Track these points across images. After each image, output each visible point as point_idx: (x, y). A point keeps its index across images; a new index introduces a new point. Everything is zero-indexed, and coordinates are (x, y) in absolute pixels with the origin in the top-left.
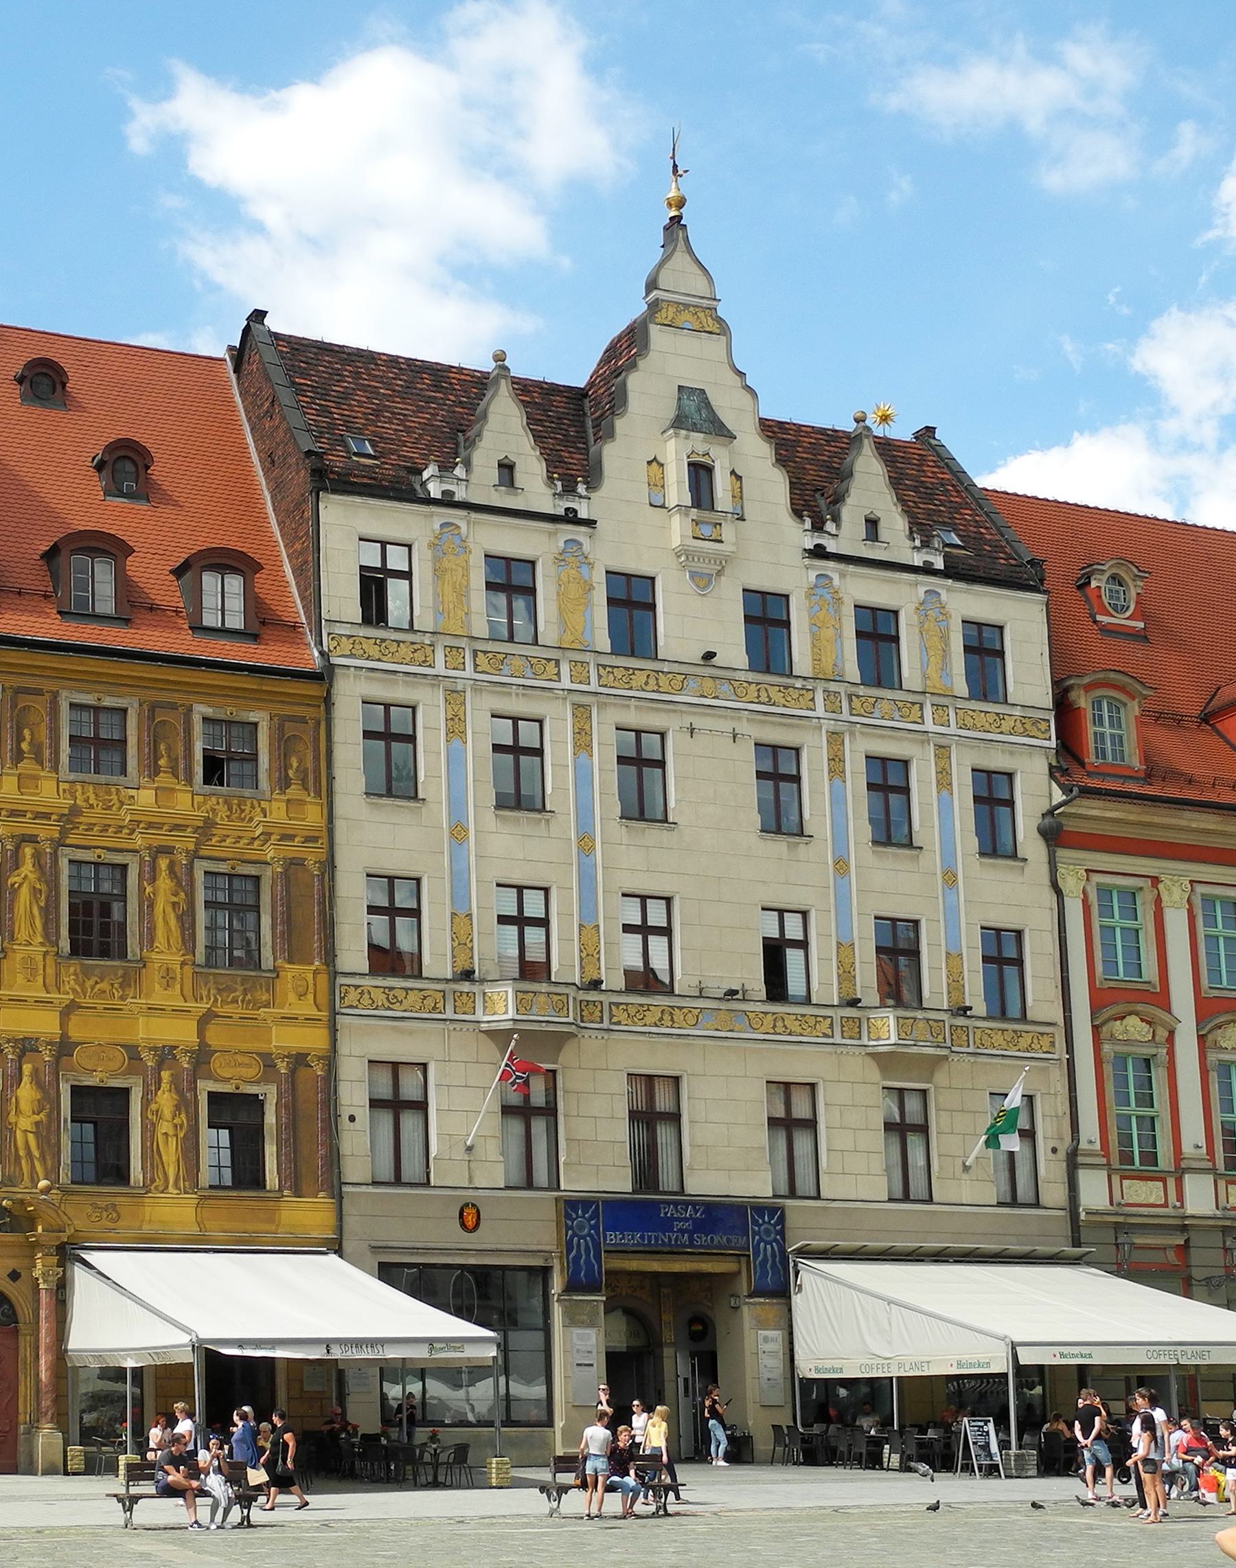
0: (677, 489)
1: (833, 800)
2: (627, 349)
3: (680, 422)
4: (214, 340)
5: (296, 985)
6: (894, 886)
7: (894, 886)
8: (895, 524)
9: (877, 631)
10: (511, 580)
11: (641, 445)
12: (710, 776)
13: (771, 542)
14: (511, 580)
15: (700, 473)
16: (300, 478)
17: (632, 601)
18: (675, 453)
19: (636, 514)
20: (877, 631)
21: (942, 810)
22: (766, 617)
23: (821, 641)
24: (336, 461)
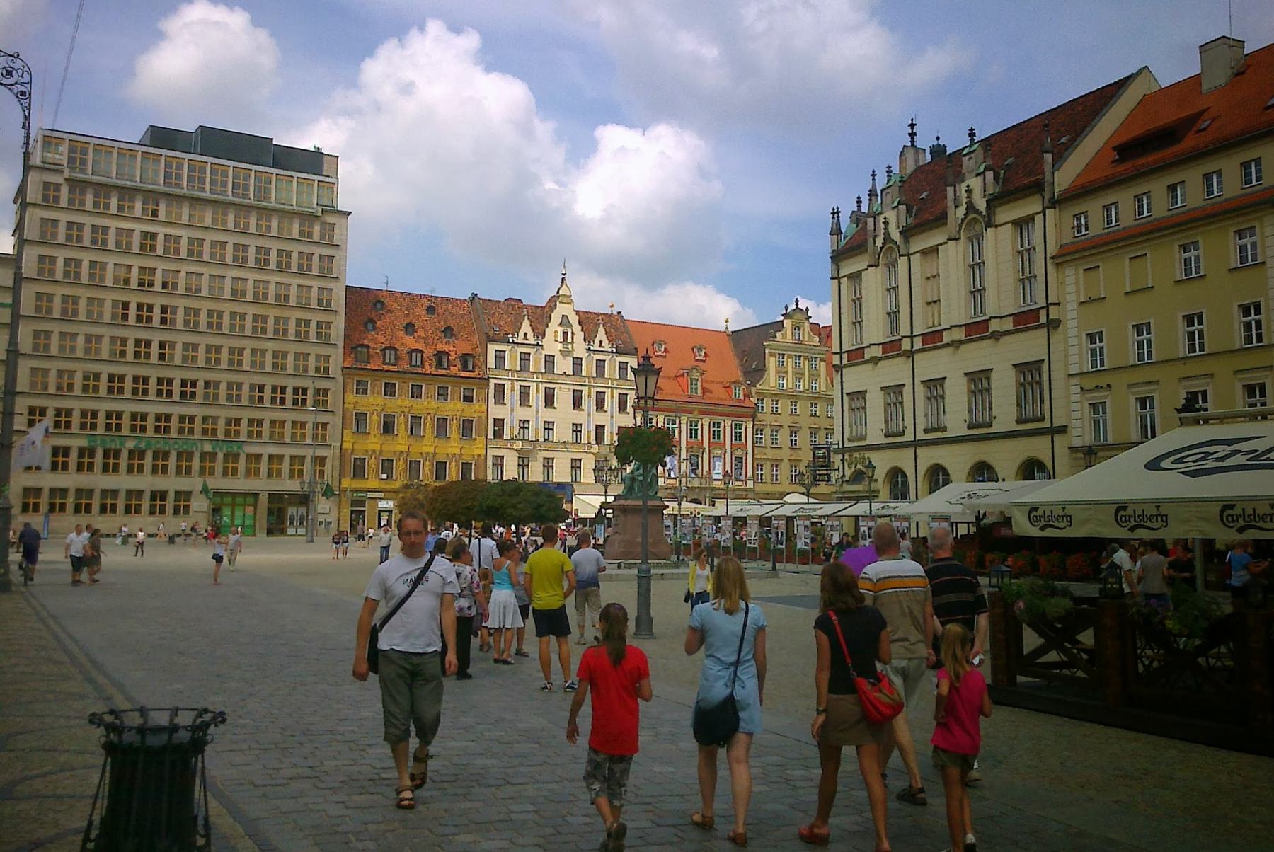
0: (560, 339)
1: (588, 402)
2: (553, 301)
3: (561, 324)
4: (466, 296)
5: (480, 441)
6: (600, 418)
7: (600, 418)
8: (605, 343)
9: (600, 365)
10: (525, 358)
11: (554, 328)
12: (563, 398)
13: (580, 348)
14: (525, 358)
15: (565, 334)
16: (484, 337)
17: (549, 360)
18: (560, 330)
19: (551, 344)
20: (600, 365)
21: (611, 403)
22: (577, 363)
23: (588, 368)
24: (491, 333)
